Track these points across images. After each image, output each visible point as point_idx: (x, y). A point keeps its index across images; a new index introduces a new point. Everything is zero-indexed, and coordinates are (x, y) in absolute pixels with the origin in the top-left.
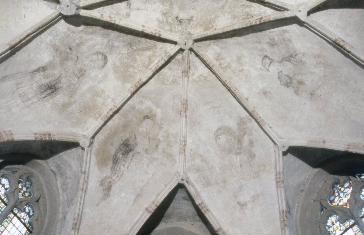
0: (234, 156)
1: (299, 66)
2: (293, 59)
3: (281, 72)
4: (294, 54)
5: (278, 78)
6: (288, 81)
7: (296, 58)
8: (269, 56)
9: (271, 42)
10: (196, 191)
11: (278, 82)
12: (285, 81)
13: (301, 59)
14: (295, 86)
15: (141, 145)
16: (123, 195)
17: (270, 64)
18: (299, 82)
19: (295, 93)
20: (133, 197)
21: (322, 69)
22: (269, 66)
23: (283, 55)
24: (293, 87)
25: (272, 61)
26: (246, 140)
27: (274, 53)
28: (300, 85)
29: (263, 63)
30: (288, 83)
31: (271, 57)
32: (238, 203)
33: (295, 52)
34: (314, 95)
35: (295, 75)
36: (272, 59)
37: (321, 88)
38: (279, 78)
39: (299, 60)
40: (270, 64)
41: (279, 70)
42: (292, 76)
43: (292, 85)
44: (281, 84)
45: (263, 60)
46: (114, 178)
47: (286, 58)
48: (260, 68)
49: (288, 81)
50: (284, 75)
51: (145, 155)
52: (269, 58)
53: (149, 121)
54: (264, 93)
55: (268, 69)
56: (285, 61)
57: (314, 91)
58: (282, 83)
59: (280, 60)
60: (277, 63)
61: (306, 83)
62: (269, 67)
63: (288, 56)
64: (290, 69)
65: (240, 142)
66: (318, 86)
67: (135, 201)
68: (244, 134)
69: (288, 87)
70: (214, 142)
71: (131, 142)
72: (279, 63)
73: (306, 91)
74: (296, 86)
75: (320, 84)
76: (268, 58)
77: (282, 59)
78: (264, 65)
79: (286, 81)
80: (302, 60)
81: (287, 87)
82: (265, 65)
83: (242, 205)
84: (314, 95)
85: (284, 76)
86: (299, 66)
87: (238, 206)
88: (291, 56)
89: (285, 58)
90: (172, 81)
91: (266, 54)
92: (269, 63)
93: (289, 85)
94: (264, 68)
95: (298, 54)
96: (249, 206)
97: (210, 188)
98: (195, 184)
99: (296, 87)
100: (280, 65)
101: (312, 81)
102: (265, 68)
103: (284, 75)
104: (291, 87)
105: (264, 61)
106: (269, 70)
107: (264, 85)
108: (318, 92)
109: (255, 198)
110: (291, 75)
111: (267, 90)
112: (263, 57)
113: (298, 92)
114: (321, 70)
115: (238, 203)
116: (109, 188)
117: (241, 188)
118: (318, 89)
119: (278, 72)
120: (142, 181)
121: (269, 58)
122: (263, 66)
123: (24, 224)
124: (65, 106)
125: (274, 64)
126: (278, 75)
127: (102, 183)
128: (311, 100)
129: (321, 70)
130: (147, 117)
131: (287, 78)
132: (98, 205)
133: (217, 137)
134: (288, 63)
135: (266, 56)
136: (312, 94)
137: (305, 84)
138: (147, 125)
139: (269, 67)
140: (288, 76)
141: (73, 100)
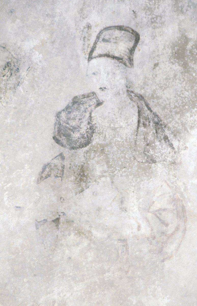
1: (135, 159)
2: (151, 130)
3: (99, 104)
4: (167, 133)
5: (76, 97)
6: (76, 135)
7: (157, 143)
8: (139, 46)
9: (189, 47)
11: (62, 104)
12: (73, 123)
13: (157, 160)
14: (66, 163)
17: (114, 57)
18: (83, 171)
19: (44, 169)
21: (145, 231)
22: (108, 56)
23: (158, 98)
24: (62, 156)
25: (128, 64)
27: (156, 65)
28: (73, 178)
29: (110, 32)
30: (68, 136)
31: (137, 55)
33: (175, 136)
34: (58, 229)
35: (103, 151)
36: (131, 60)
37: (85, 243)
38: (76, 101)
39: (151, 152)
40: (114, 57)
41: (101, 96)
42: (94, 143)
43: (66, 152)
44: (58, 115)
45: (120, 28)
47: (149, 109)
48: (89, 27)
49: (76, 135)
50: (90, 116)
52: (132, 51)
54: (8, 64)
55: (95, 54)
56: (136, 109)
57: (70, 222)
58: (63, 115)
59: (137, 91)
60: (123, 82)
61: (87, 192)
62: (100, 56)
63: (156, 115)
64: (114, 129)
66: (90, 232)
69: (57, 141)
72: (125, 89)
73: (61, 199)
74: (66, 163)
75: (98, 234)
76: (131, 44)
77: (141, 97)
78: (106, 35)
79: (74, 129)
80: (154, 162)
81: (54, 138)
82: (104, 40)
84: (58, 229)
85: (87, 115)
86: (135, 159)
88: (159, 125)
89: (147, 105)
91: (145, 36)
92: (117, 55)
93: (63, 140)
94: (93, 39)
95: (171, 146)
99: (63, 167)
100: (119, 94)
101: (99, 209)
102: (95, 43)
103: (90, 116)
104: (58, 149)
105: (117, 33)
106: (90, 58)
107: (37, 57)
108: (72, 237)
110: (96, 140)
111: (23, 73)
112: (132, 25)
113: (49, 175)
114: (139, 228)
118: (79, 232)
119: (94, 93)
121: (132, 51)
122: (101, 32)
125: (118, 72)
126: (84, 96)
128: (38, 224)
129: (139, 228)
131: (84, 128)
134: (135, 119)
135: (137, 38)
136: (57, 221)
137: (82, 191)
139: (100, 56)
140: (92, 129)
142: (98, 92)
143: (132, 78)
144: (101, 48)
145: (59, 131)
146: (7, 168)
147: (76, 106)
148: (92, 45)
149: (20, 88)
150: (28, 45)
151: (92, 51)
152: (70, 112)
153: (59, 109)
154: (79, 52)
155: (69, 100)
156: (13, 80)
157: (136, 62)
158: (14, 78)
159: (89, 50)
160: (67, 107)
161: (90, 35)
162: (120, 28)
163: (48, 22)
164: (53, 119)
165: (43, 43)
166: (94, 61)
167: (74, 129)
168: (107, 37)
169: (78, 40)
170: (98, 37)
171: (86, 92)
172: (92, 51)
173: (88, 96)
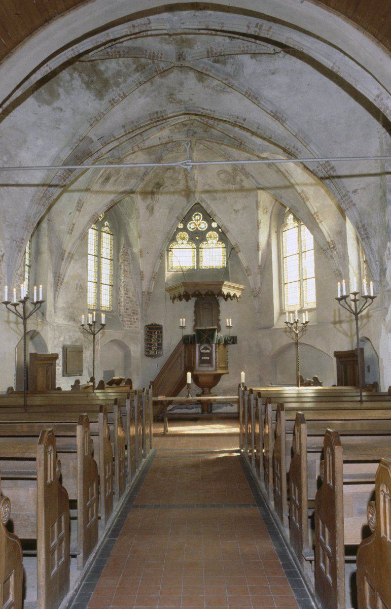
0: (231, 185)
10: (208, 205)
15: (168, 183)
16: (161, 210)
20: (168, 211)
26: (238, 178)
32: (234, 210)
46: (154, 203)
51: (171, 187)
53: (172, 171)
65: (234, 178)
67: (169, 212)
68: (236, 176)
70: (217, 177)
71: (161, 182)
83: (236, 211)
87: (234, 212)
90: (184, 151)
96: (240, 212)
97: (216, 201)
98: (206, 200)
109: (244, 208)
115: (234, 210)
116: (153, 209)
117: (236, 202)
120: (172, 201)
123: (108, 233)
124: (116, 181)
127: (147, 208)
130: (170, 169)
132: (148, 220)
133: (218, 175)
138: (169, 174)
141: (119, 175)
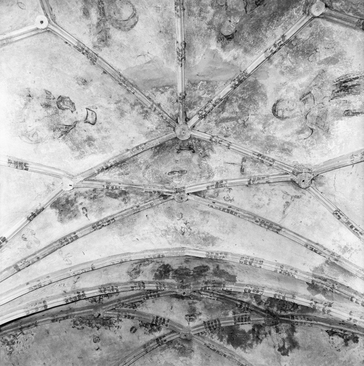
3: (72, 112)
5: (74, 104)
8: (91, 125)
12: (66, 103)
17: (87, 116)
22: (87, 115)
27: (85, 131)
30: (61, 101)
31: (88, 124)
36: (86, 122)
38: (73, 104)
40: (87, 116)
41: (75, 112)
44: (68, 98)
45: (96, 119)
48: (96, 108)
52: (89, 123)
55: (88, 110)
58: (68, 99)
62: (87, 112)
69: (59, 97)
76: (91, 122)
78: (94, 114)
79: (64, 103)
82: (92, 113)
85: (68, 108)
93: (60, 99)
94: (93, 110)
102: (91, 110)
104: (57, 97)
105: (95, 118)
106: (87, 109)
107: (88, 91)
111: (83, 86)
119: (75, 110)
121: (89, 123)
122: (94, 112)
126: (75, 106)
135: (93, 124)
139: (87, 112)
142: (76, 111)
143: (81, 123)
144: (90, 112)
145: (63, 98)
146: (49, 79)
147: (71, 104)
148: (91, 109)
149: (78, 85)
150: (91, 88)
151: (89, 109)
152: (69, 102)
153: (70, 98)
154: (89, 105)
155: (73, 101)
156: (80, 82)
157: (86, 124)
158: (81, 83)
159: (89, 108)
160: (71, 101)
161: (94, 109)
162: (96, 119)
163: (99, 95)
164: (67, 96)
165: (92, 93)
166: (86, 110)
167: (64, 103)
168: (93, 114)
169: (92, 105)
170: (93, 111)
171: (76, 107)
172: (89, 109)
173: (74, 108)
